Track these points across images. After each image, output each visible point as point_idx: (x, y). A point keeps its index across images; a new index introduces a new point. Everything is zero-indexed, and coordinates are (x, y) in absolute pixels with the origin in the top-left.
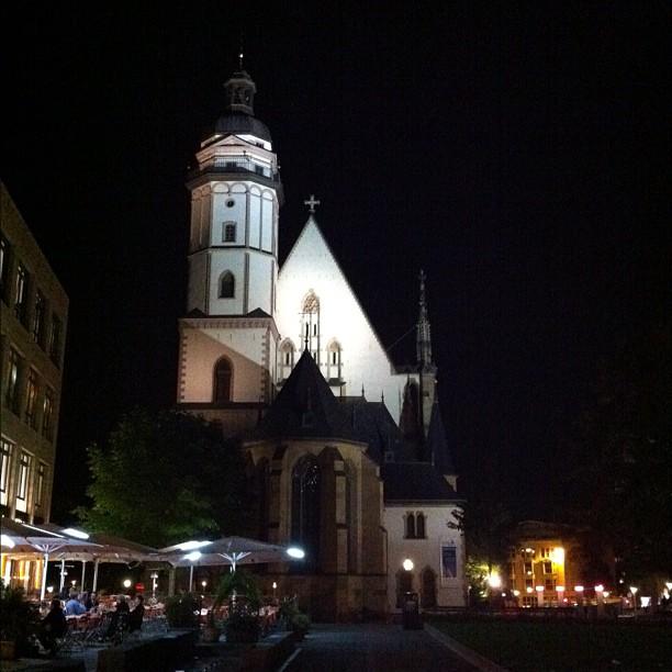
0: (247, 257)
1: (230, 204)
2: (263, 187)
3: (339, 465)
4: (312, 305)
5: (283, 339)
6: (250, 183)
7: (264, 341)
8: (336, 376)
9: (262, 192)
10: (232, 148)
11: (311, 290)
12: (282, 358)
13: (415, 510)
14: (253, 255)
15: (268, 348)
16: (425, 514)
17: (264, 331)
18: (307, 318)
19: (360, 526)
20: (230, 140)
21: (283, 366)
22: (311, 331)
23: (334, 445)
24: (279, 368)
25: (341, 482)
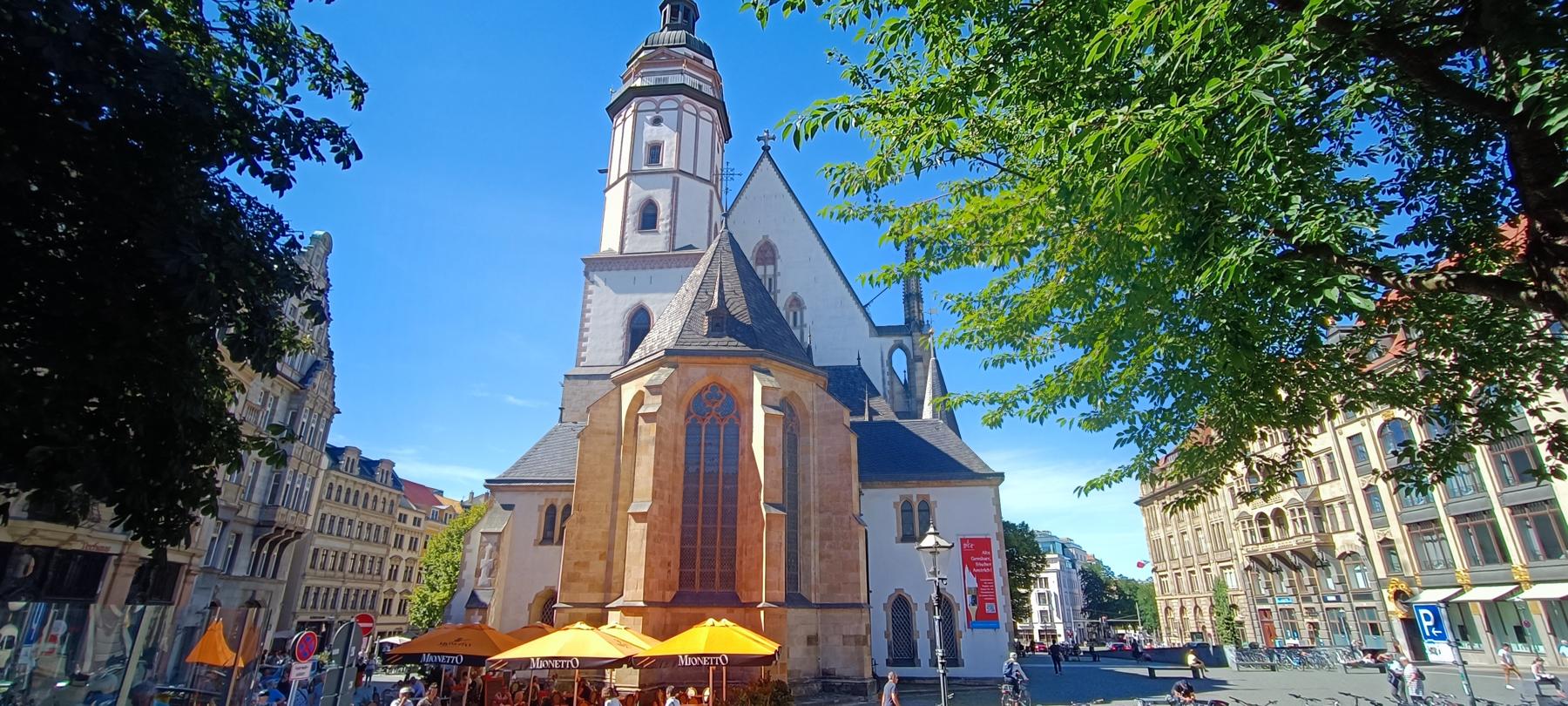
0: (676, 183)
2: (700, 105)
13: (914, 492)
14: (683, 179)
16: (932, 499)
19: (815, 518)
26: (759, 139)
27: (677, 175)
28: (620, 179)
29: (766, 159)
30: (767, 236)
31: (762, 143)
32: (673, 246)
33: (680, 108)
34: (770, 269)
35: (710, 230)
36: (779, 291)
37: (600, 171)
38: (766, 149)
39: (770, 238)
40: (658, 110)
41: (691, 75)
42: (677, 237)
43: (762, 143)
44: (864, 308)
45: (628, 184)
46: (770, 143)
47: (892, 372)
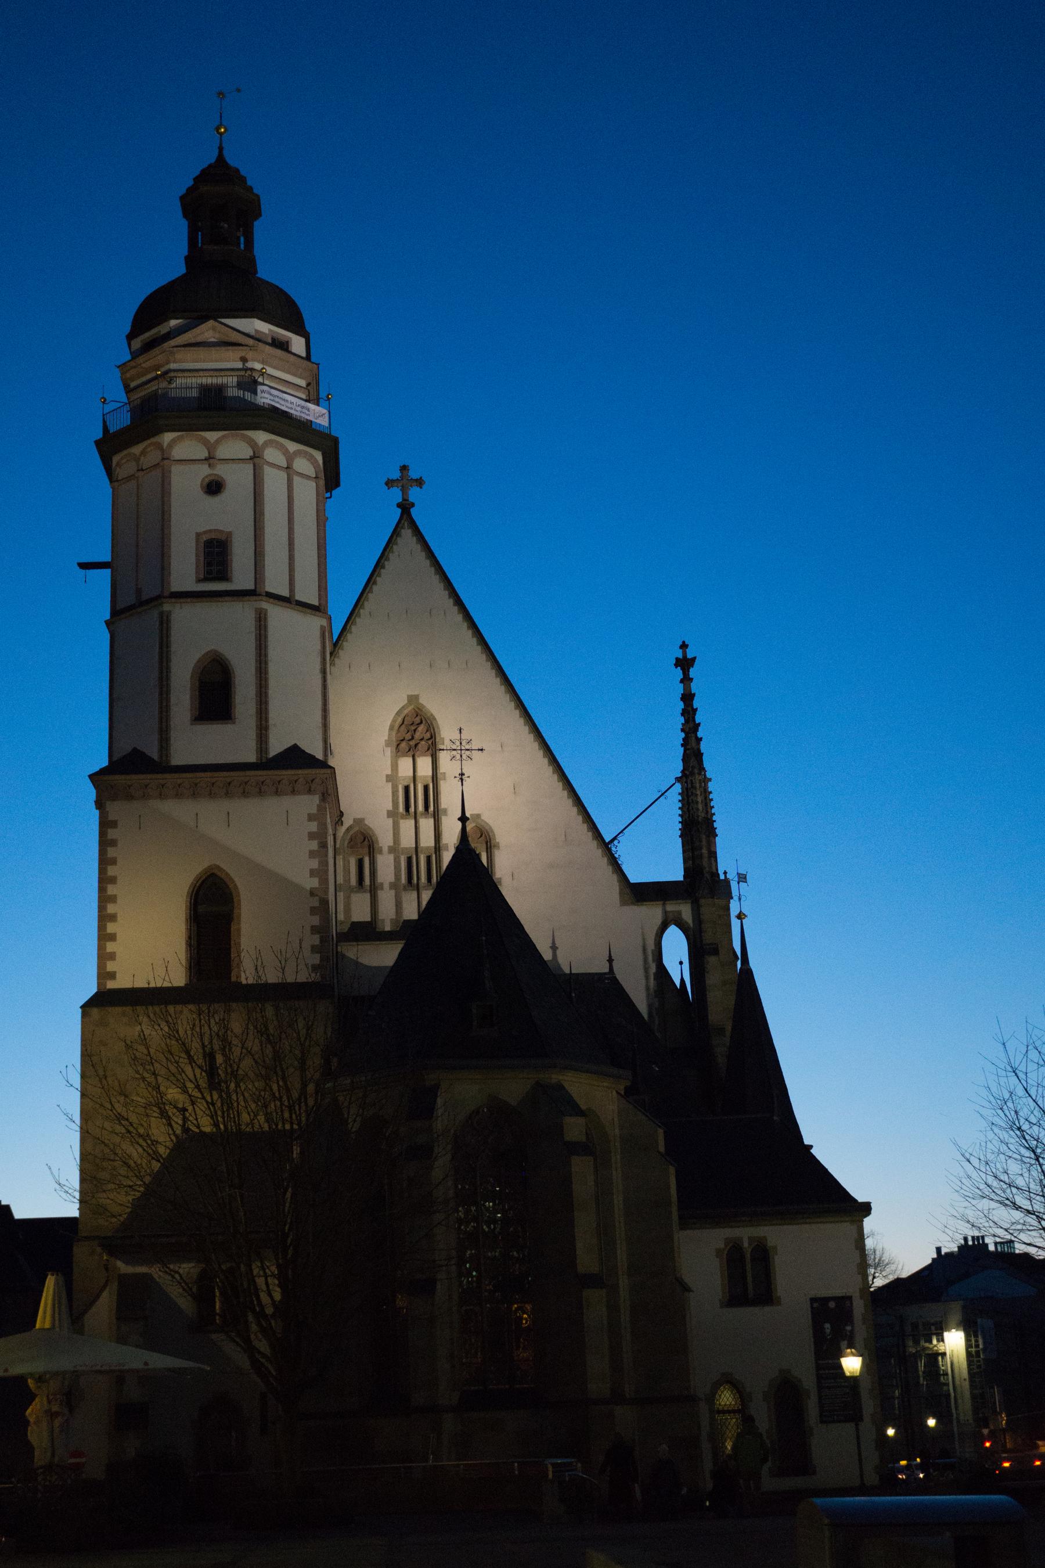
0: (261, 620)
2: (292, 446)
3: (574, 1129)
5: (348, 821)
6: (261, 437)
7: (313, 827)
9: (290, 458)
10: (214, 352)
12: (347, 871)
14: (278, 616)
15: (323, 845)
16: (771, 1243)
17: (309, 803)
18: (405, 766)
20: (207, 331)
21: (351, 890)
23: (555, 1077)
24: (341, 895)
25: (581, 1167)
26: (389, 483)
29: (407, 533)
30: (417, 697)
31: (396, 495)
33: (256, 458)
37: (84, 566)
38: (406, 507)
40: (210, 460)
43: (396, 495)
44: (606, 847)
47: (662, 972)
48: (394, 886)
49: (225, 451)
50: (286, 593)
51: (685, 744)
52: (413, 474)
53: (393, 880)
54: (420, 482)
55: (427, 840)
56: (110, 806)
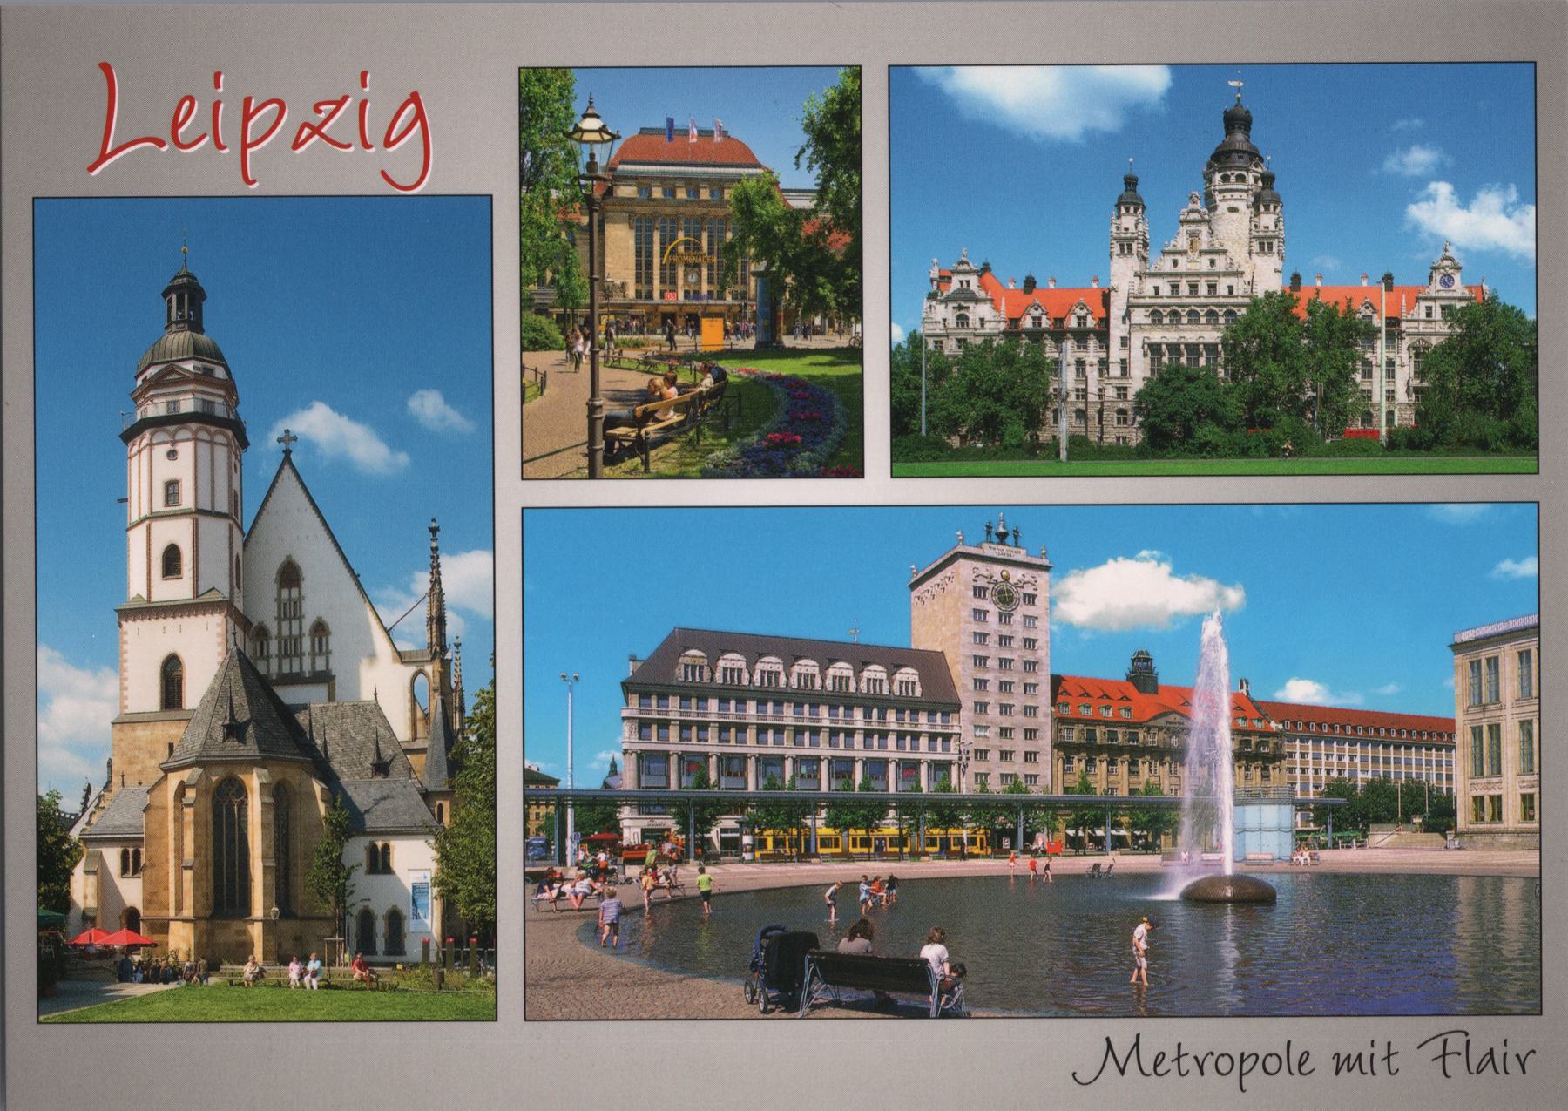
1: (172, 455)
2: (213, 429)
4: (290, 575)
8: (324, 669)
11: (289, 557)
12: (255, 650)
14: (205, 522)
18: (285, 593)
22: (290, 611)
27: (196, 516)
28: (142, 521)
32: (197, 592)
34: (295, 592)
35: (231, 563)
36: (304, 617)
38: (287, 453)
39: (294, 558)
41: (203, 392)
42: (201, 583)
45: (149, 528)
46: (292, 445)
48: (277, 656)
49: (180, 435)
50: (209, 508)
51: (432, 573)
52: (292, 435)
53: (277, 652)
54: (295, 439)
55: (295, 631)
56: (123, 623)
